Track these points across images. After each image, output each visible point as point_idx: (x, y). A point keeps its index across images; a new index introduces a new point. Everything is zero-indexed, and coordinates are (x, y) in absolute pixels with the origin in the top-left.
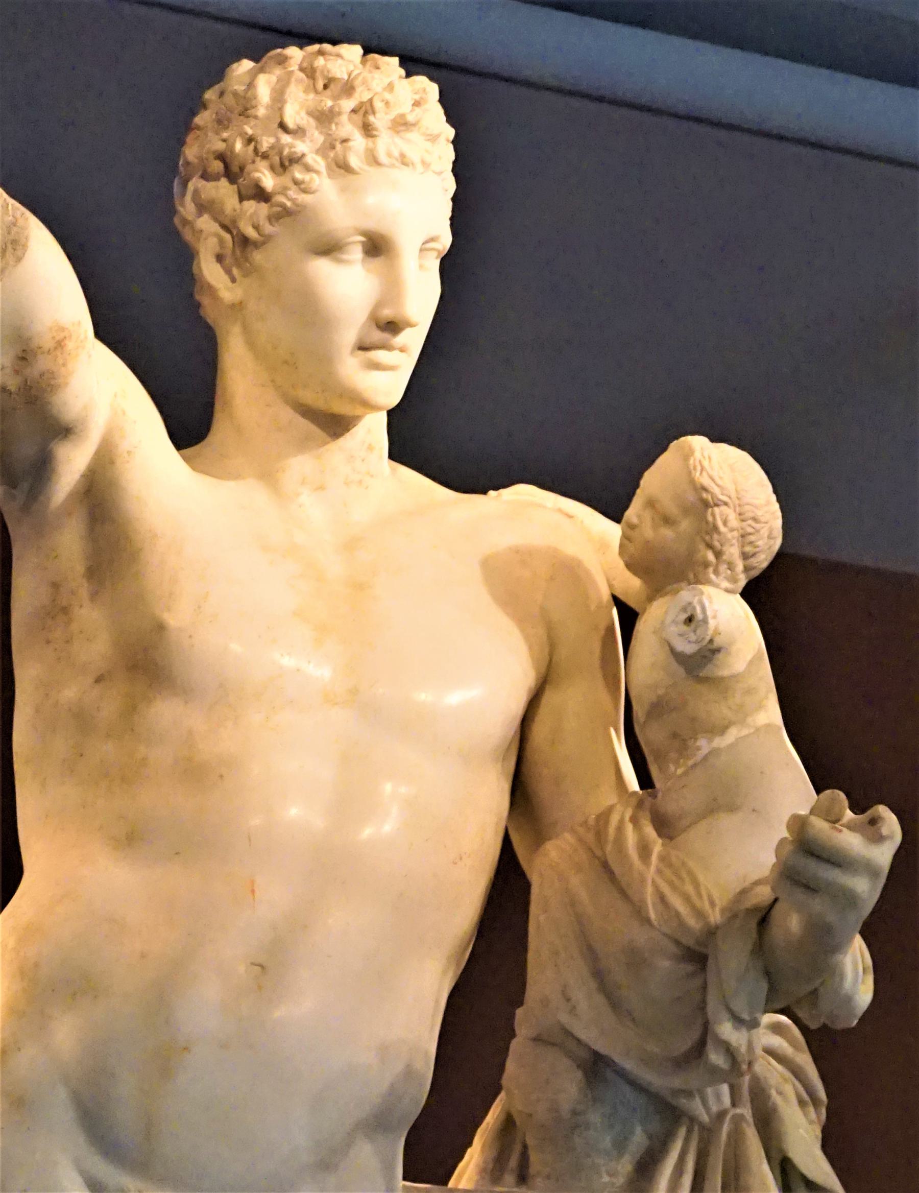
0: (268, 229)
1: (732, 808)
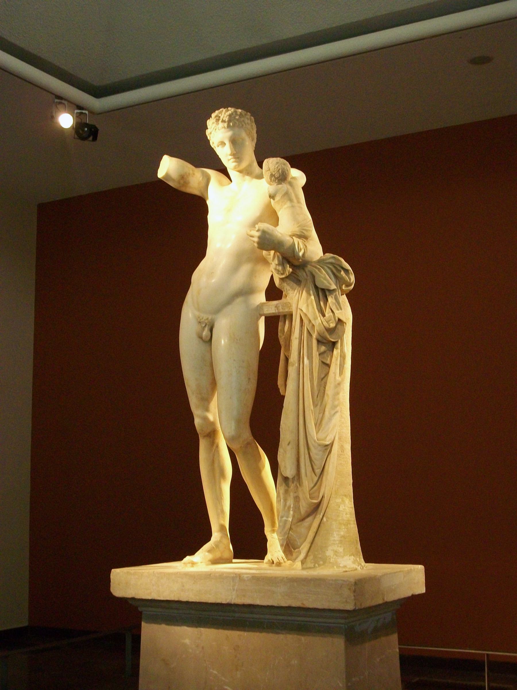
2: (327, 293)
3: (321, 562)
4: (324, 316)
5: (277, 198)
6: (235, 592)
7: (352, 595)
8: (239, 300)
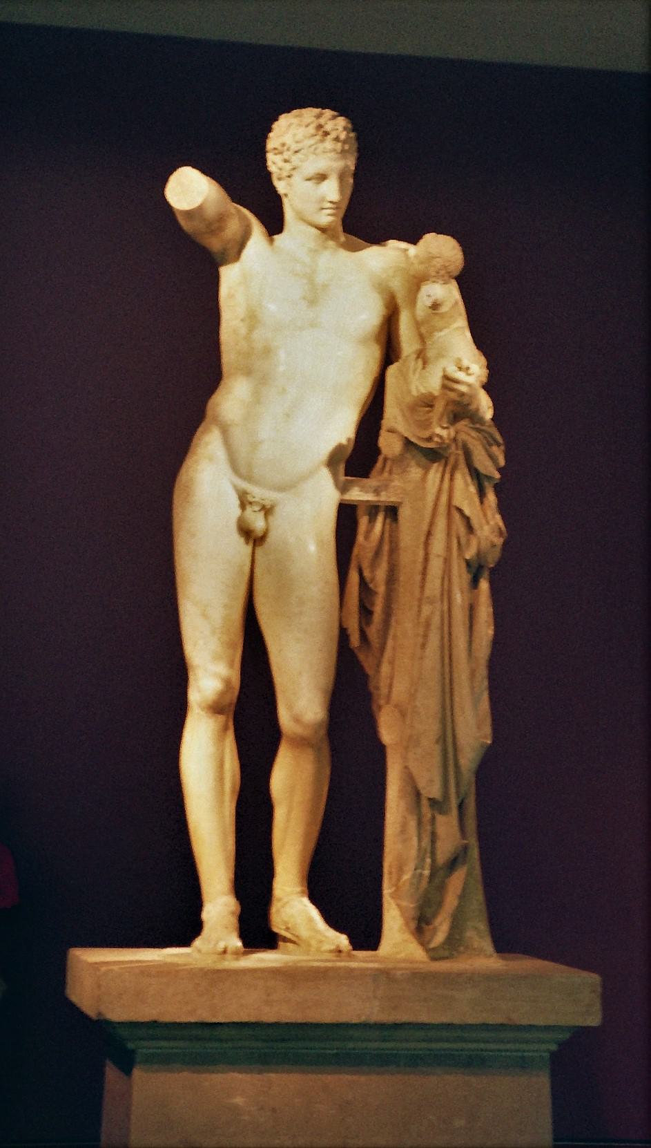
1: (443, 356)
2: (486, 484)
4: (488, 523)
6: (377, 1003)
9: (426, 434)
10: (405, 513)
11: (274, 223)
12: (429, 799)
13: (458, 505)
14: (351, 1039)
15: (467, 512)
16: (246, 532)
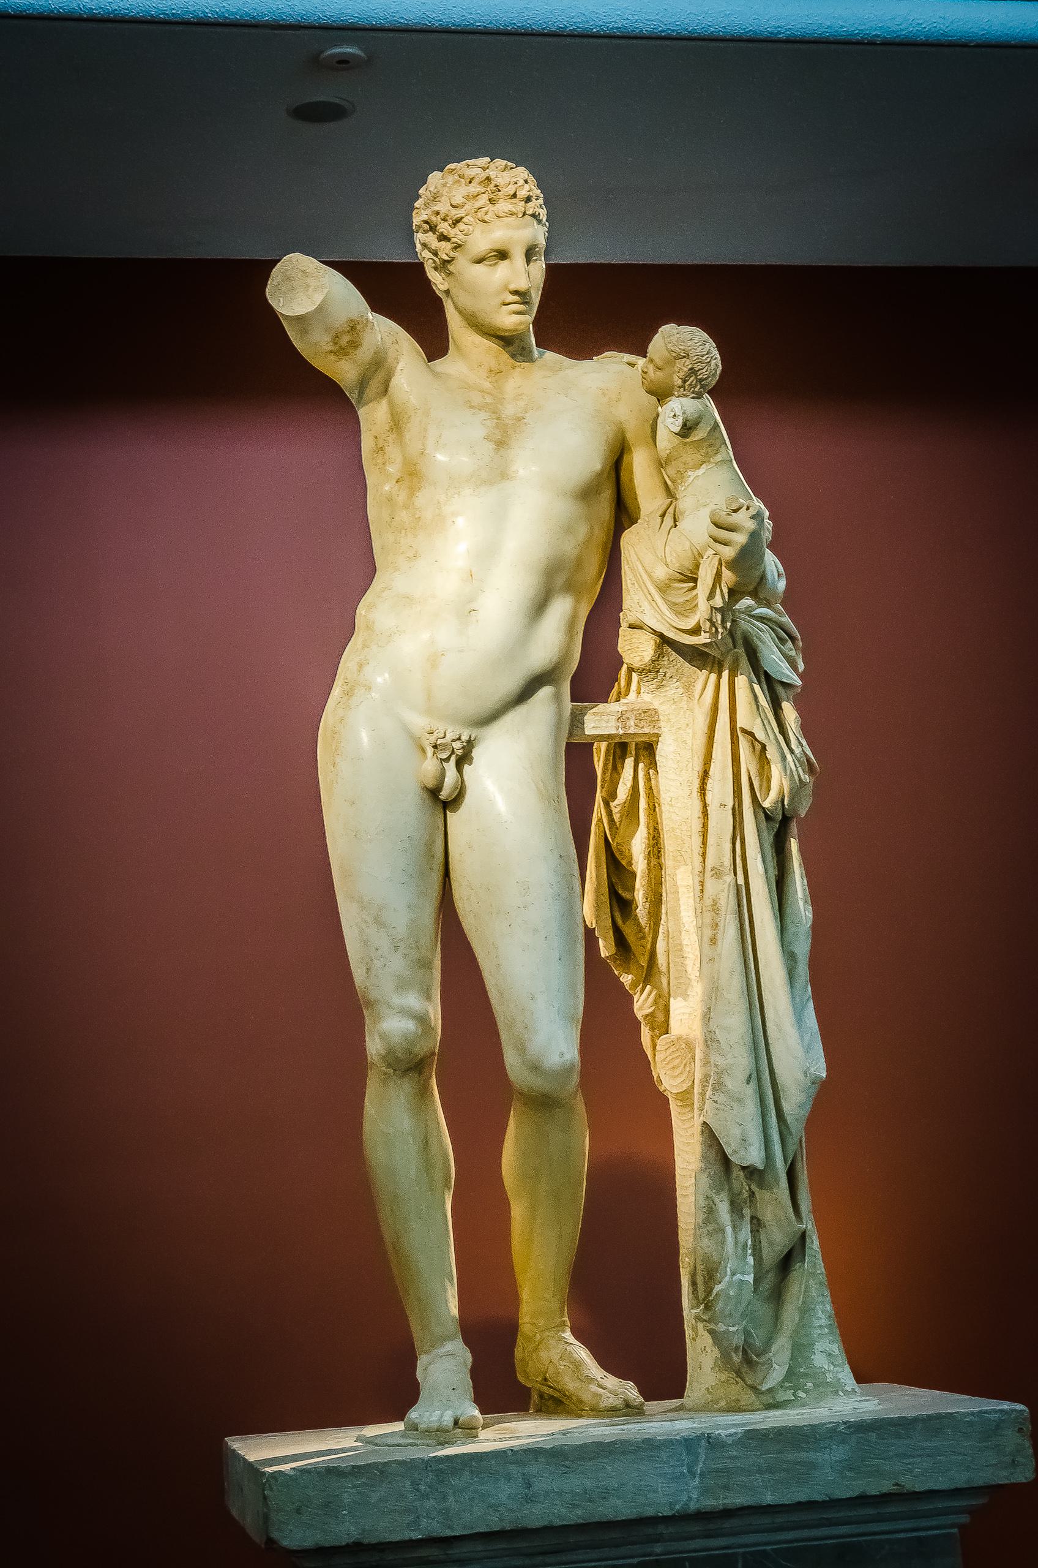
0: (452, 254)
3: (810, 1385)
4: (792, 751)
5: (699, 435)
7: (1027, 1444)
8: (546, 692)
9: (690, 624)
10: (664, 751)
11: (435, 343)
12: (744, 1168)
13: (749, 729)
14: (659, 1539)
15: (760, 735)
16: (434, 792)
